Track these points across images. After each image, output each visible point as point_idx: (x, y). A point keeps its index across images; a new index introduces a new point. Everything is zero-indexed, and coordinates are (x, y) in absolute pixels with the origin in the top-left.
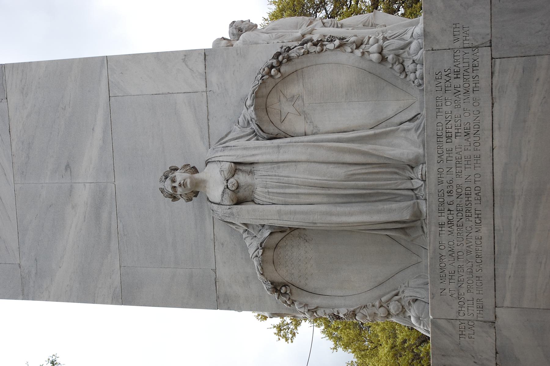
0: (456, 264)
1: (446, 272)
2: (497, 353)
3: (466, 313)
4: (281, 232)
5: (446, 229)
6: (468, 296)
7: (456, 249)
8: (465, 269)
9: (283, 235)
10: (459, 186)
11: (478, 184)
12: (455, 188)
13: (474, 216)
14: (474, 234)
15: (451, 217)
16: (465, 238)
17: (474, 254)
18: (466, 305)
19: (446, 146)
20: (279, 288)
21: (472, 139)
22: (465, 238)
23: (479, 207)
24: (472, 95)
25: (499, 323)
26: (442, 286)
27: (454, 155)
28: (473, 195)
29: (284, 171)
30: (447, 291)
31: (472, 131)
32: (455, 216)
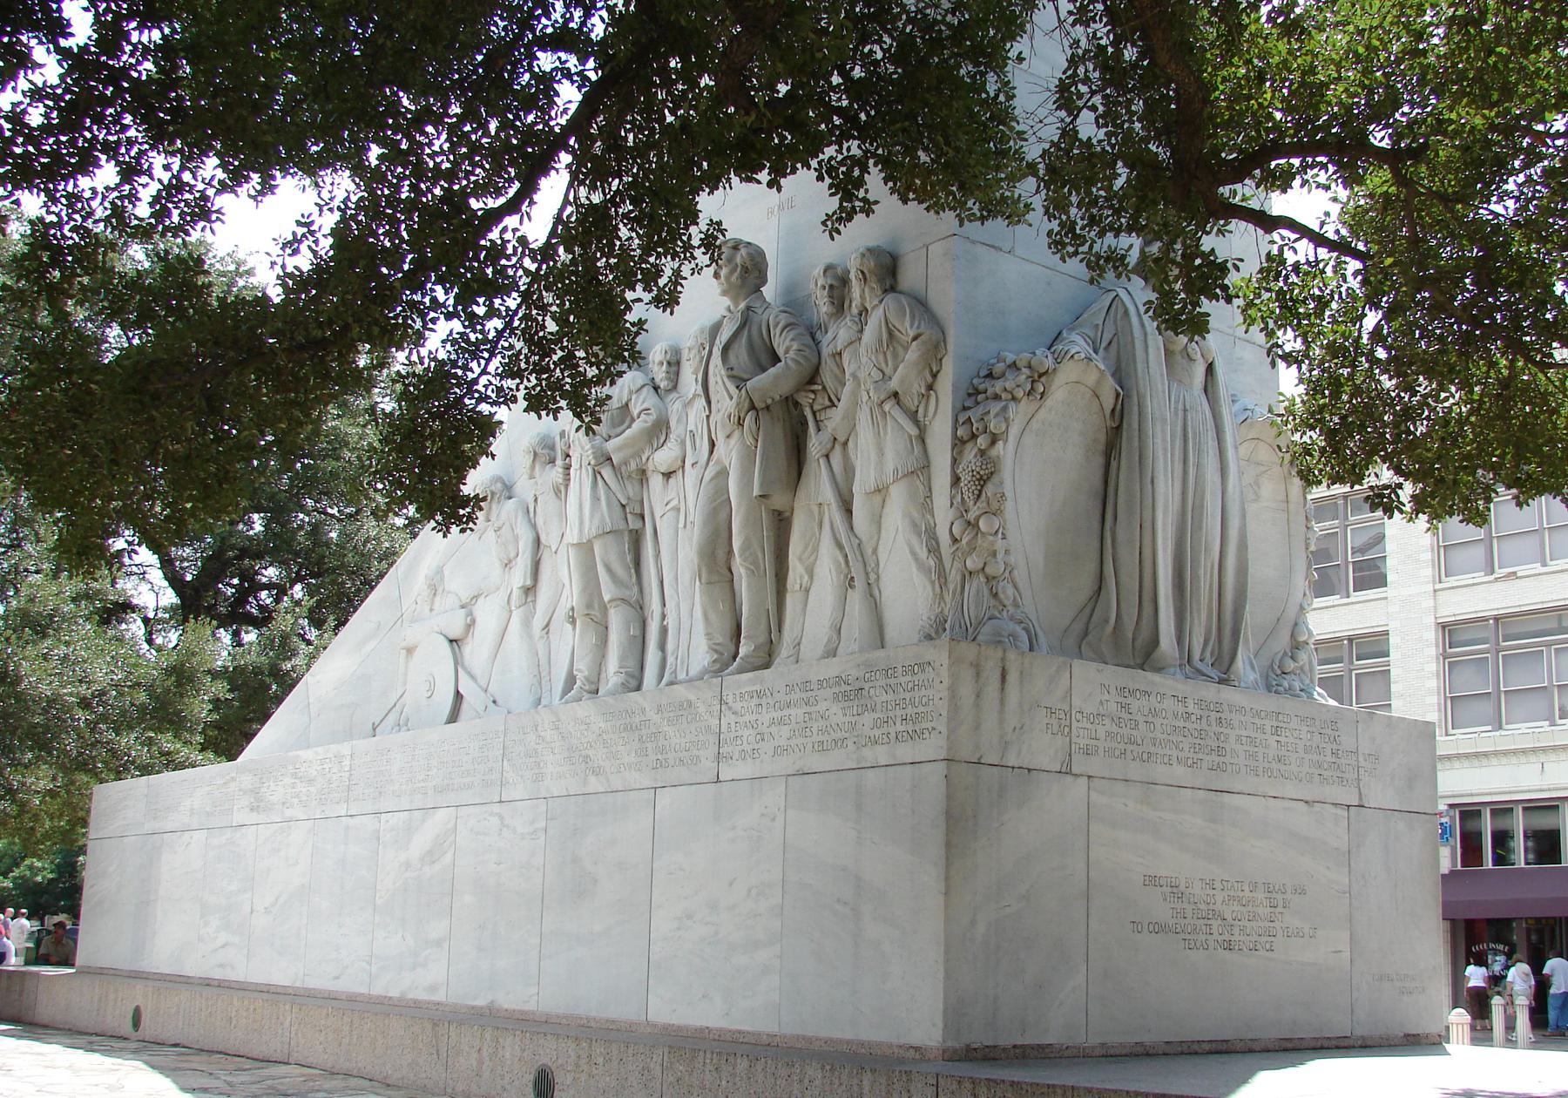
0: (1141, 719)
1: (1129, 700)
2: (1029, 770)
3: (1080, 724)
4: (1113, 410)
5: (1181, 709)
6: (1101, 733)
7: (1158, 721)
8: (1134, 732)
9: (1108, 412)
10: (1227, 736)
11: (1229, 767)
12: (1226, 731)
13: (1195, 756)
14: (1175, 753)
15: (1193, 718)
16: (1170, 738)
17: (1152, 749)
18: (1089, 726)
19: (1268, 724)
20: (1043, 379)
21: (1274, 766)
22: (1170, 738)
23: (1205, 765)
24: (1317, 772)
25: (1069, 779)
26: (1113, 690)
27: (1260, 736)
28: (1217, 759)
29: (1211, 444)
30: (1106, 696)
31: (1283, 768)
32: (1195, 726)
